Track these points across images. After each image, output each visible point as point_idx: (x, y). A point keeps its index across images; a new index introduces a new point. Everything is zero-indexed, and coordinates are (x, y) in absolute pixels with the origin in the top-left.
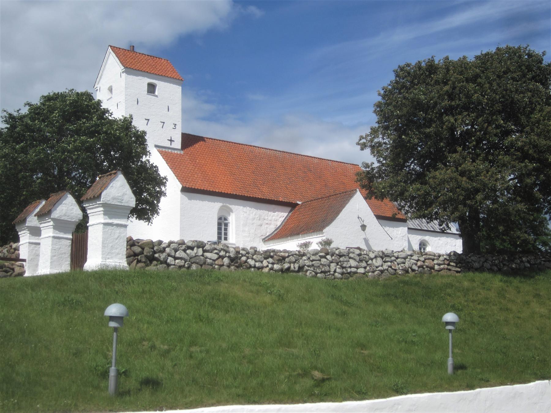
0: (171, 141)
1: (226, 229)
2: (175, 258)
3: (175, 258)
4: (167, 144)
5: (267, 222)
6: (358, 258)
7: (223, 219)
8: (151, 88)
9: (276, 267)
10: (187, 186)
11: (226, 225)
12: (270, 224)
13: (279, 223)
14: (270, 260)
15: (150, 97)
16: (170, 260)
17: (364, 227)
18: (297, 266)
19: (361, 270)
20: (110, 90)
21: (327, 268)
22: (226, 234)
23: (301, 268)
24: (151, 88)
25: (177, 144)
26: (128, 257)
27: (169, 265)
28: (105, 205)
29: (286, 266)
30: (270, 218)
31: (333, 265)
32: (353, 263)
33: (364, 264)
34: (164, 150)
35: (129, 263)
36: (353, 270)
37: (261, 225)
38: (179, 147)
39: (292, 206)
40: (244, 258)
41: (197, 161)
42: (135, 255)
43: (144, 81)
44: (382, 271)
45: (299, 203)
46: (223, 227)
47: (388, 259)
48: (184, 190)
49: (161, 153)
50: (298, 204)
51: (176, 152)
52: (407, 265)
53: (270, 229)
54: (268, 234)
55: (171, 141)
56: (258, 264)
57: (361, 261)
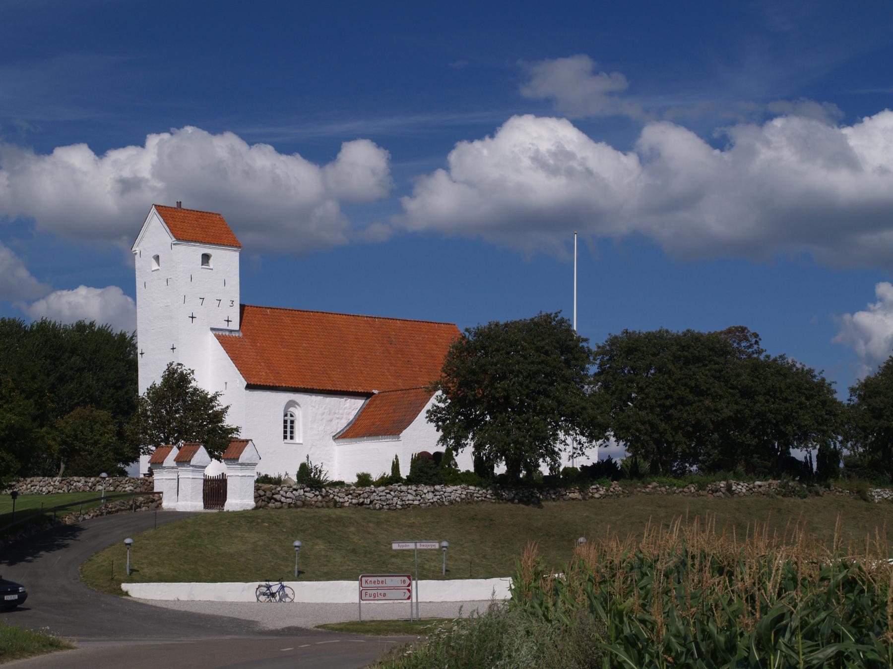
1: (292, 427)
2: (287, 498)
3: (287, 498)
4: (224, 326)
6: (414, 493)
8: (206, 258)
9: (354, 501)
11: (292, 422)
12: (342, 418)
13: (351, 417)
14: (350, 496)
16: (283, 499)
18: (369, 500)
19: (416, 503)
21: (391, 502)
22: (292, 432)
23: (371, 502)
24: (206, 258)
26: (255, 498)
27: (282, 503)
28: (242, 464)
29: (361, 500)
30: (341, 412)
31: (395, 499)
32: (410, 497)
33: (419, 498)
35: (256, 502)
36: (411, 502)
37: (331, 420)
38: (237, 328)
39: (367, 395)
40: (331, 496)
42: (260, 496)
43: (198, 250)
44: (432, 503)
45: (376, 392)
46: (289, 425)
47: (437, 493)
49: (218, 337)
50: (373, 394)
52: (453, 497)
53: (341, 424)
56: (341, 500)
57: (417, 495)
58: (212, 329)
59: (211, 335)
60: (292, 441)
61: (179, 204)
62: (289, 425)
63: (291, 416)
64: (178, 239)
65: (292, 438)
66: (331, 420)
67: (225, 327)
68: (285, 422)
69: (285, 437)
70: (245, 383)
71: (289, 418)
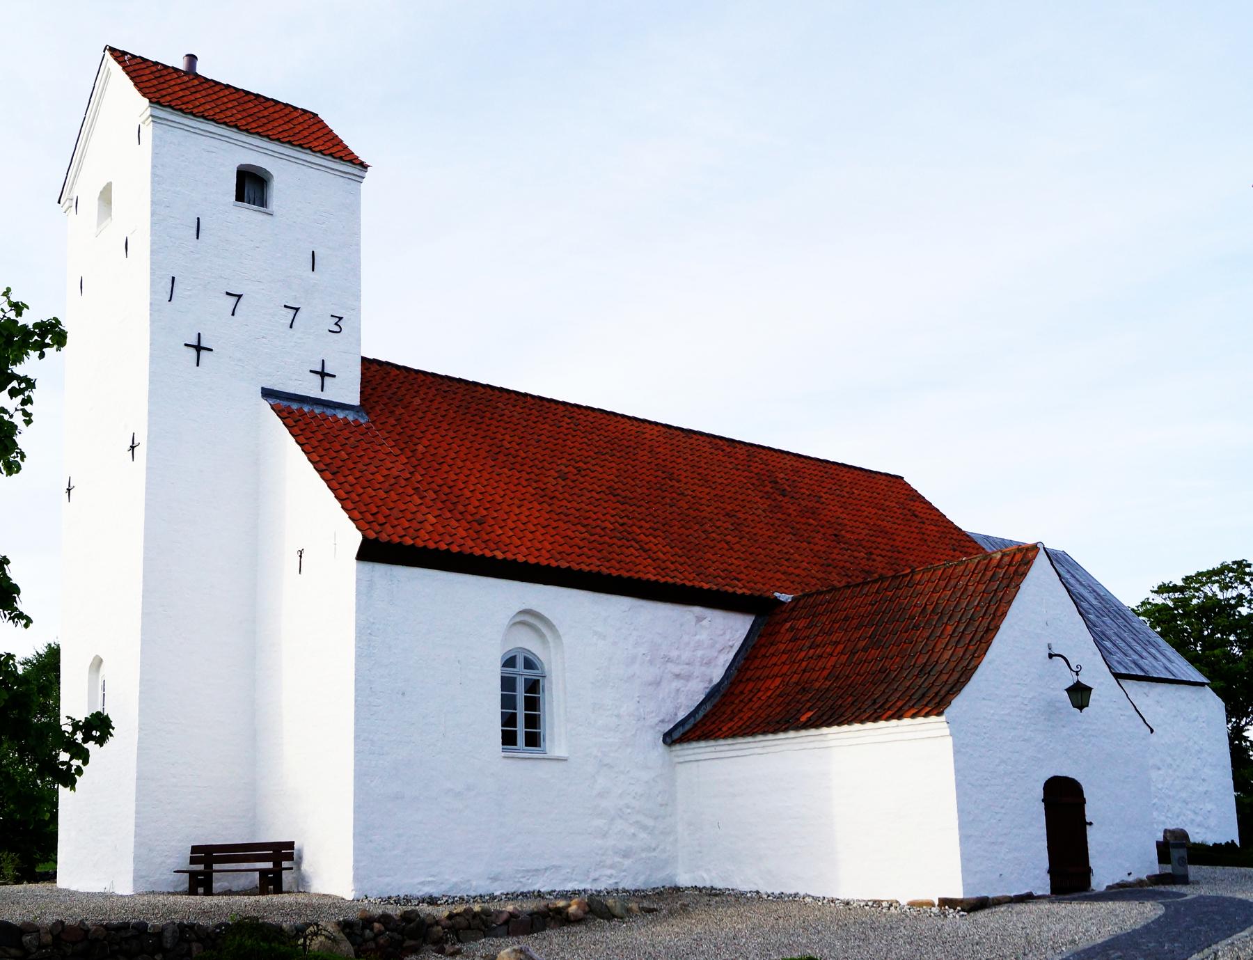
0: (323, 374)
4: (309, 387)
5: (677, 670)
7: (520, 662)
8: (252, 186)
10: (384, 538)
11: (533, 686)
12: (688, 678)
13: (717, 674)
15: (247, 214)
17: (1079, 694)
20: (106, 196)
22: (533, 721)
24: (252, 186)
25: (346, 389)
30: (686, 655)
34: (295, 406)
37: (657, 683)
38: (354, 398)
41: (420, 448)
45: (785, 597)
48: (369, 552)
51: (341, 415)
53: (688, 696)
54: (682, 715)
55: (323, 374)
58: (267, 393)
59: (265, 406)
60: (532, 752)
61: (192, 59)
62: (520, 694)
63: (529, 664)
64: (155, 102)
65: (533, 740)
66: (657, 683)
67: (315, 393)
68: (508, 684)
69: (509, 739)
70: (356, 538)
71: (521, 674)
